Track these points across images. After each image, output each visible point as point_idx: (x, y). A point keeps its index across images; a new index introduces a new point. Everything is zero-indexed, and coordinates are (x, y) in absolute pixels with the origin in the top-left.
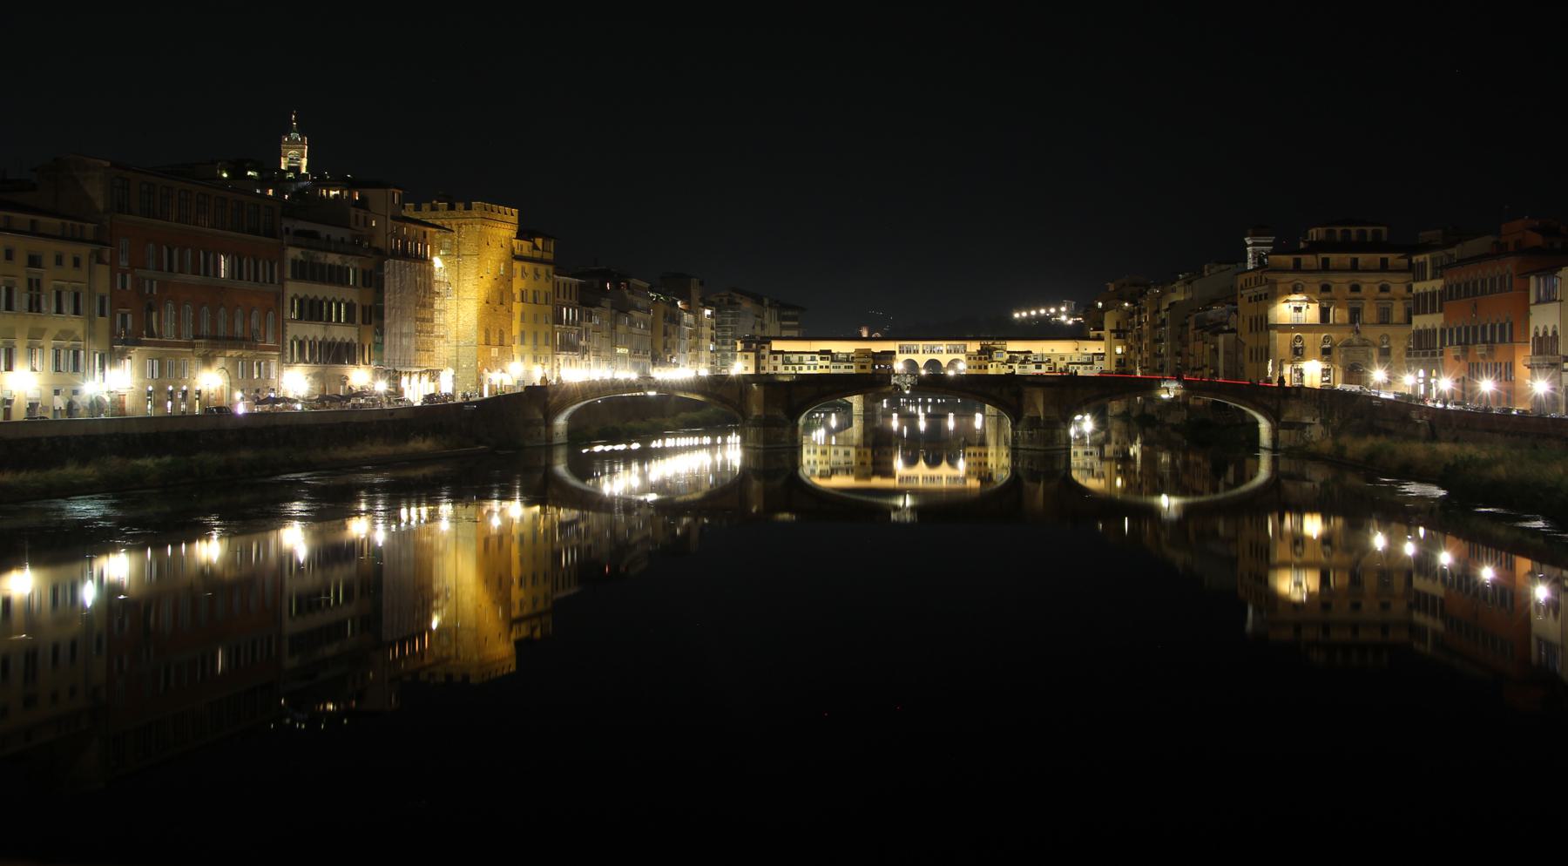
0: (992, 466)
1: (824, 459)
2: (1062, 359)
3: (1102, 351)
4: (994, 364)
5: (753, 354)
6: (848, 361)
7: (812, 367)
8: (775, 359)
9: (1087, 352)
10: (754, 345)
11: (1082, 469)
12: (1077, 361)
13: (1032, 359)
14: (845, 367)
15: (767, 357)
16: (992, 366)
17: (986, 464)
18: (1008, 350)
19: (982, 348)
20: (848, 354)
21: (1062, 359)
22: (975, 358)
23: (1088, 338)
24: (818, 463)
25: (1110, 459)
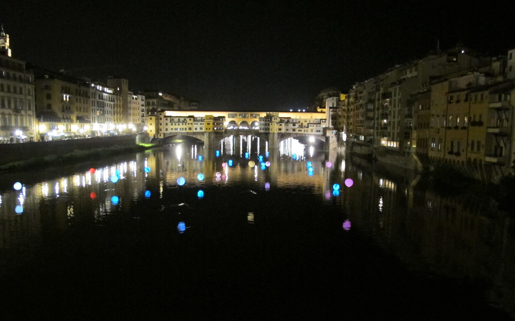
2: (306, 121)
5: (154, 117)
6: (202, 121)
8: (167, 120)
9: (316, 118)
10: (156, 113)
12: (313, 123)
13: (291, 121)
14: (200, 124)
15: (162, 119)
16: (272, 124)
19: (267, 115)
20: (202, 118)
21: (306, 121)
22: (263, 120)
23: (316, 112)
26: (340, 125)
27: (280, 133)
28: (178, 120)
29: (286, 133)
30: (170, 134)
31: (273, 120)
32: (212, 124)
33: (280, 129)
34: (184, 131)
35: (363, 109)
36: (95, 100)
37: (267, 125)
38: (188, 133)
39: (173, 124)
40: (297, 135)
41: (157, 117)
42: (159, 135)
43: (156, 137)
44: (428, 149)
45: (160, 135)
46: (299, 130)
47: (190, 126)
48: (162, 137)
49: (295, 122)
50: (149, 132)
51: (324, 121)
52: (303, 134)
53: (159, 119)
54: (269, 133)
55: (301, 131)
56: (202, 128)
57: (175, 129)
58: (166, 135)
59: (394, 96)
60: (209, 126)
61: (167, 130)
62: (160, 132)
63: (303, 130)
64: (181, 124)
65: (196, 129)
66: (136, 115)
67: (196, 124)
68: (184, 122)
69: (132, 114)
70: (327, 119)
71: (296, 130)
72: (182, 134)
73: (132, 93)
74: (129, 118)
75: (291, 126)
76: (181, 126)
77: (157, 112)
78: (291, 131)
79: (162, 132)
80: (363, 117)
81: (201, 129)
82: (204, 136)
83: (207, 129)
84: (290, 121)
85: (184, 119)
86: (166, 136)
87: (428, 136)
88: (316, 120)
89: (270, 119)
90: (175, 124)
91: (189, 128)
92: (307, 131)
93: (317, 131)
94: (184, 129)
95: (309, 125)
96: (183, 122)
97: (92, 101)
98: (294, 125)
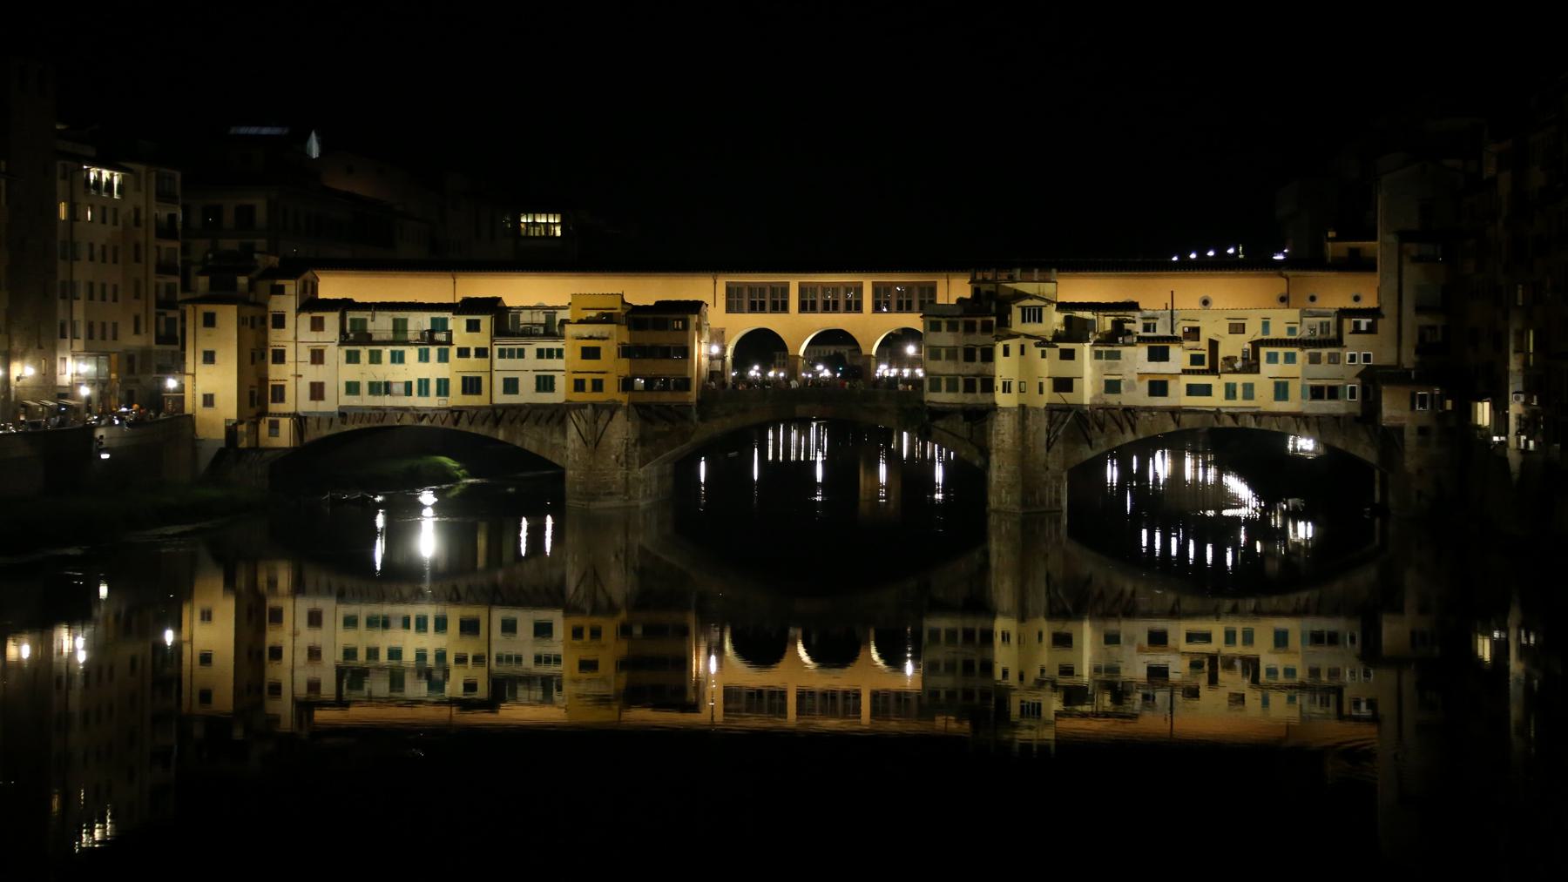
0: (1005, 673)
1: (470, 647)
3: (1369, 302)
4: (1014, 344)
8: (317, 325)
11: (1302, 687)
12: (1284, 335)
13: (1138, 328)
14: (540, 354)
16: (1006, 352)
17: (988, 667)
18: (1059, 301)
19: (976, 291)
20: (550, 311)
21: (1237, 328)
22: (953, 327)
24: (451, 659)
25: (1396, 662)
27: (1067, 408)
28: (395, 331)
29: (1107, 409)
30: (337, 421)
31: (1016, 324)
32: (615, 350)
33: (1064, 384)
34: (432, 401)
37: (978, 353)
38: (457, 412)
39: (358, 353)
40: (1178, 423)
41: (250, 311)
42: (264, 428)
43: (243, 444)
46: (1192, 390)
47: (473, 365)
48: (285, 437)
49: (1168, 334)
50: (193, 403)
51: (1364, 323)
52: (1218, 410)
53: (264, 320)
54: (993, 408)
55: (1206, 390)
56: (552, 378)
57: (375, 388)
58: (312, 423)
60: (591, 364)
62: (274, 407)
63: (1217, 383)
65: (511, 386)
66: (109, 297)
67: (511, 355)
68: (433, 342)
69: (82, 292)
70: (1384, 311)
71: (1172, 385)
72: (422, 419)
73: (91, 152)
74: (62, 315)
75: (1136, 359)
76: (414, 368)
77: (253, 275)
78: (1138, 396)
79: (288, 406)
81: (545, 383)
82: (564, 433)
83: (579, 385)
84: (1127, 326)
85: (434, 320)
86: (312, 435)
89: (994, 319)
90: (371, 352)
91: (464, 379)
92: (1249, 390)
93: (1317, 393)
94: (433, 387)
95: (1263, 351)
96: (428, 338)
98: (1158, 354)
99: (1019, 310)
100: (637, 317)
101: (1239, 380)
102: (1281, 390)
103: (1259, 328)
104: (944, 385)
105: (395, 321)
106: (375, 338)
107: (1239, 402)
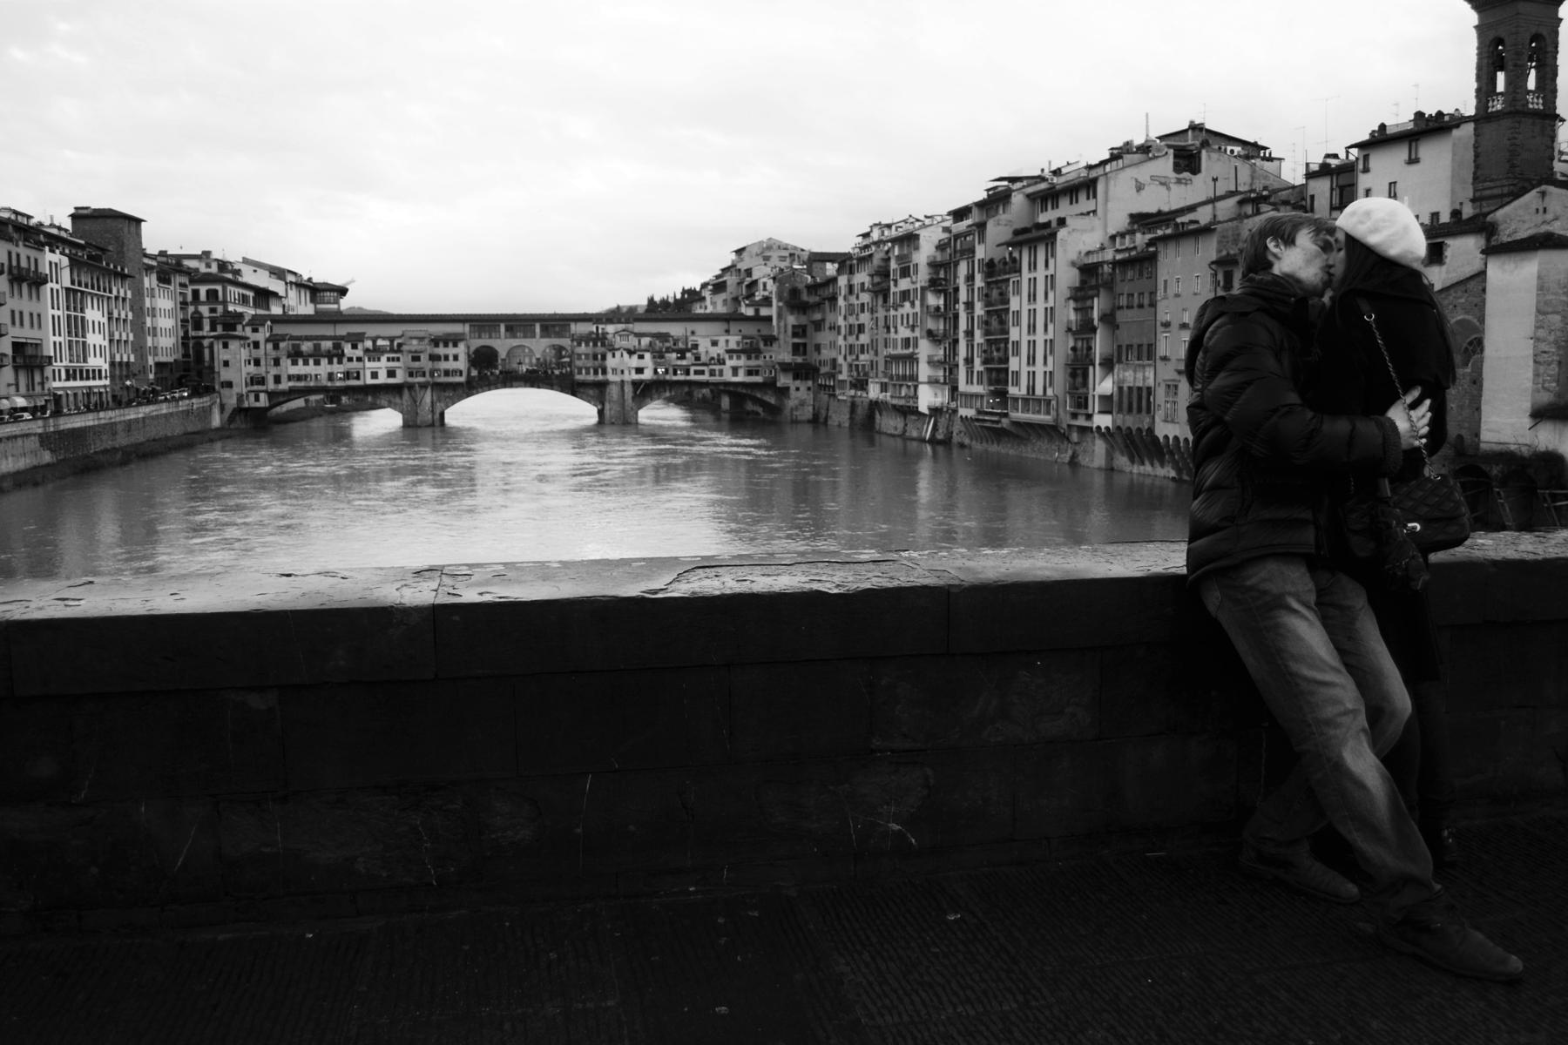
6: (392, 350)
7: (335, 360)
14: (388, 359)
20: (392, 340)
21: (715, 343)
26: (819, 353)
33: (640, 370)
35: (913, 304)
36: (58, 287)
37: (599, 356)
44: (1153, 418)
45: (257, 399)
46: (696, 373)
47: (355, 365)
48: (263, 401)
49: (684, 347)
55: (702, 373)
59: (1030, 269)
60: (417, 364)
61: (277, 379)
64: (324, 361)
65: (375, 375)
67: (374, 360)
76: (324, 368)
80: (913, 330)
82: (401, 397)
83: (411, 375)
85: (334, 344)
87: (1151, 382)
88: (745, 341)
93: (750, 373)
97: (52, 289)
99: (618, 338)
100: (436, 342)
101: (717, 368)
102: (735, 370)
103: (724, 344)
104: (584, 371)
105: (315, 345)
106: (305, 354)
107: (717, 379)
